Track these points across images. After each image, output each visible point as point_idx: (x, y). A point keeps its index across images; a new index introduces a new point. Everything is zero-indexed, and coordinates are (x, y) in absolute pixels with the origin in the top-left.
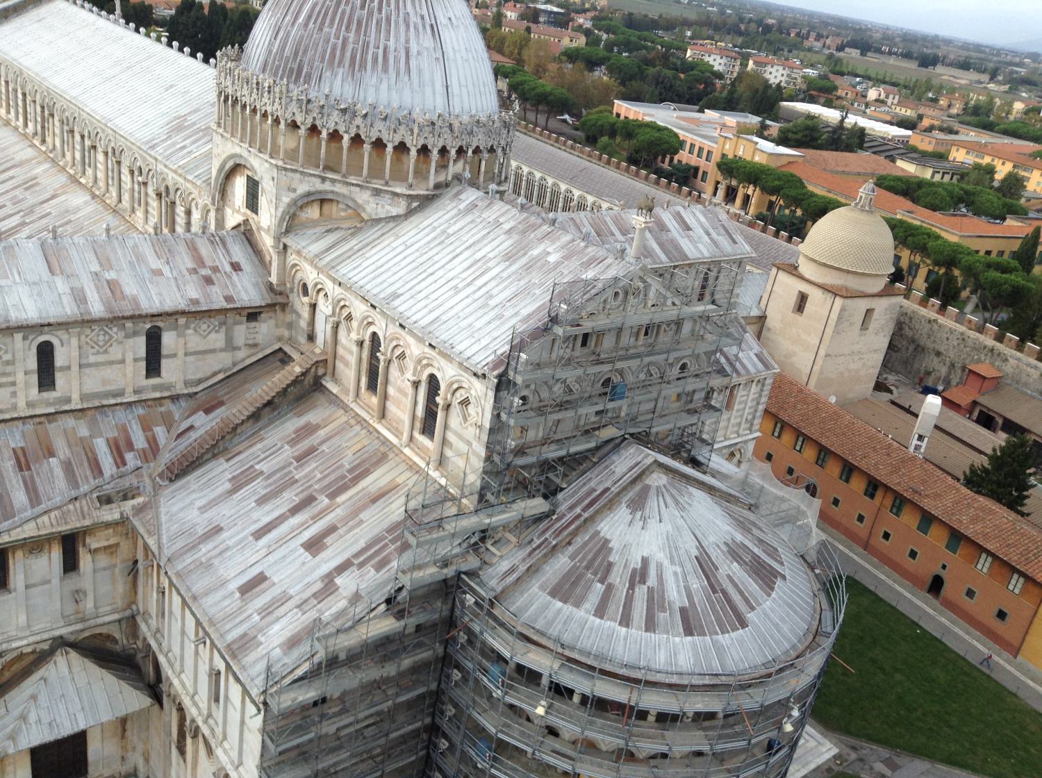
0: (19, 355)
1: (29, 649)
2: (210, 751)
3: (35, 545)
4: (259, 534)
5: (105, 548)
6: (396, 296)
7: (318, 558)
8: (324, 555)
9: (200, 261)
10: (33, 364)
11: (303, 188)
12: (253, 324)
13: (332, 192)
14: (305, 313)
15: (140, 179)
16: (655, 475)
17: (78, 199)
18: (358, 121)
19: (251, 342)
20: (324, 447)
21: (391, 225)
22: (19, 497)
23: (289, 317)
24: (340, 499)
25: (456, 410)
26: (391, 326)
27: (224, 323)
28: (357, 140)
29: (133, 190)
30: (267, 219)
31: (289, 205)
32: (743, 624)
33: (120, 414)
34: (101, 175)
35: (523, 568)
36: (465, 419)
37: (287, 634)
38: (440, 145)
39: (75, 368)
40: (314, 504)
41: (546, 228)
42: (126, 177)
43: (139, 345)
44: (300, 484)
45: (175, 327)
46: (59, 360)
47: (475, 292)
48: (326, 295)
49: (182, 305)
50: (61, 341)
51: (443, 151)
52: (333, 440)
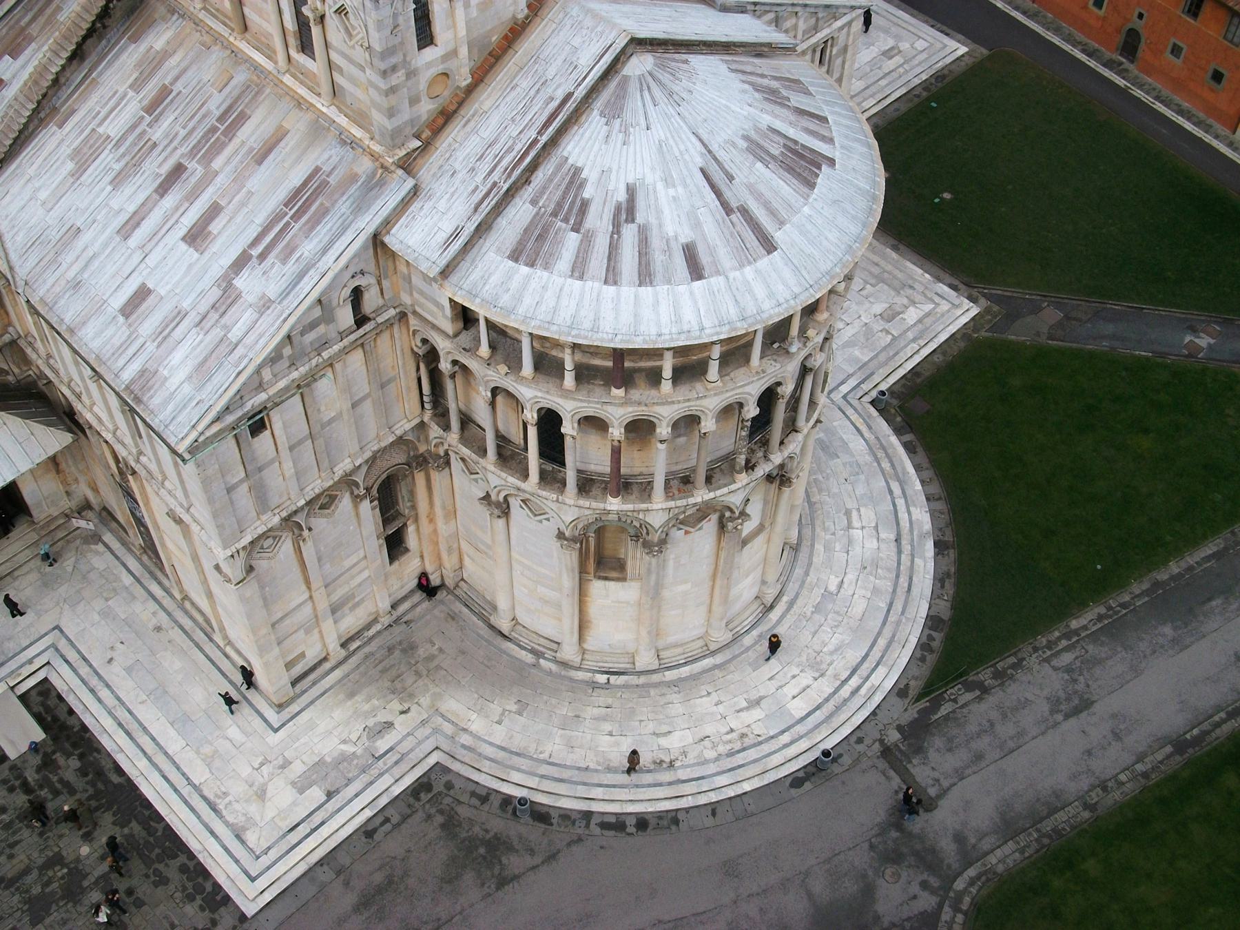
7: (207, 255)
8: (215, 247)
16: (634, 60)
20: (178, 87)
24: (217, 164)
25: (332, 21)
32: (769, 246)
35: (471, 227)
36: (350, 36)
40: (184, 176)
44: (160, 148)
52: (190, 73)
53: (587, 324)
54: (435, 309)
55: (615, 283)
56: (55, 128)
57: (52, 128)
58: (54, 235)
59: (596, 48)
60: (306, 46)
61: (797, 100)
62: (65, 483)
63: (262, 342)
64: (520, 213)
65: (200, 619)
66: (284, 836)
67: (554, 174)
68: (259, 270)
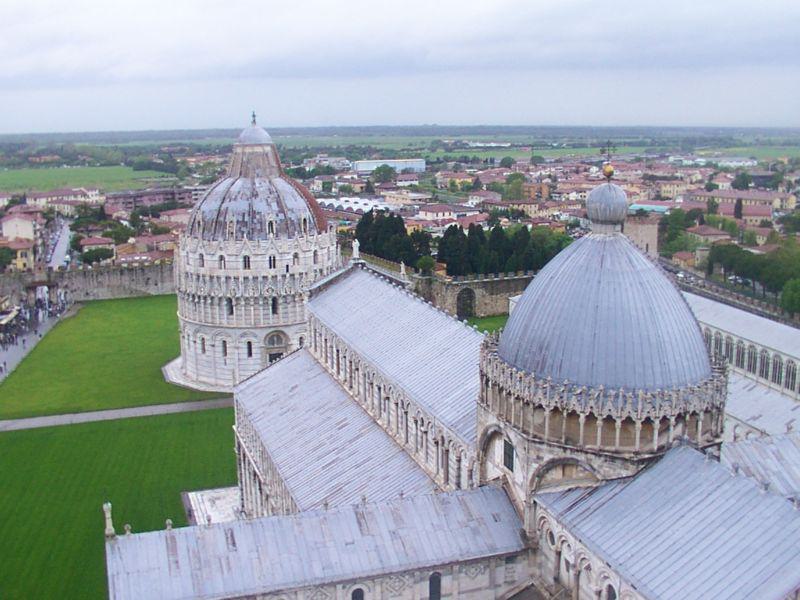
11: (547, 457)
12: (510, 566)
14: (553, 557)
15: (422, 429)
18: (592, 403)
19: (508, 579)
23: (540, 559)
26: (624, 584)
27: (488, 566)
28: (591, 418)
29: (417, 434)
30: (520, 476)
31: (538, 470)
38: (661, 416)
42: (412, 424)
48: (569, 545)
50: (369, 588)
51: (665, 420)
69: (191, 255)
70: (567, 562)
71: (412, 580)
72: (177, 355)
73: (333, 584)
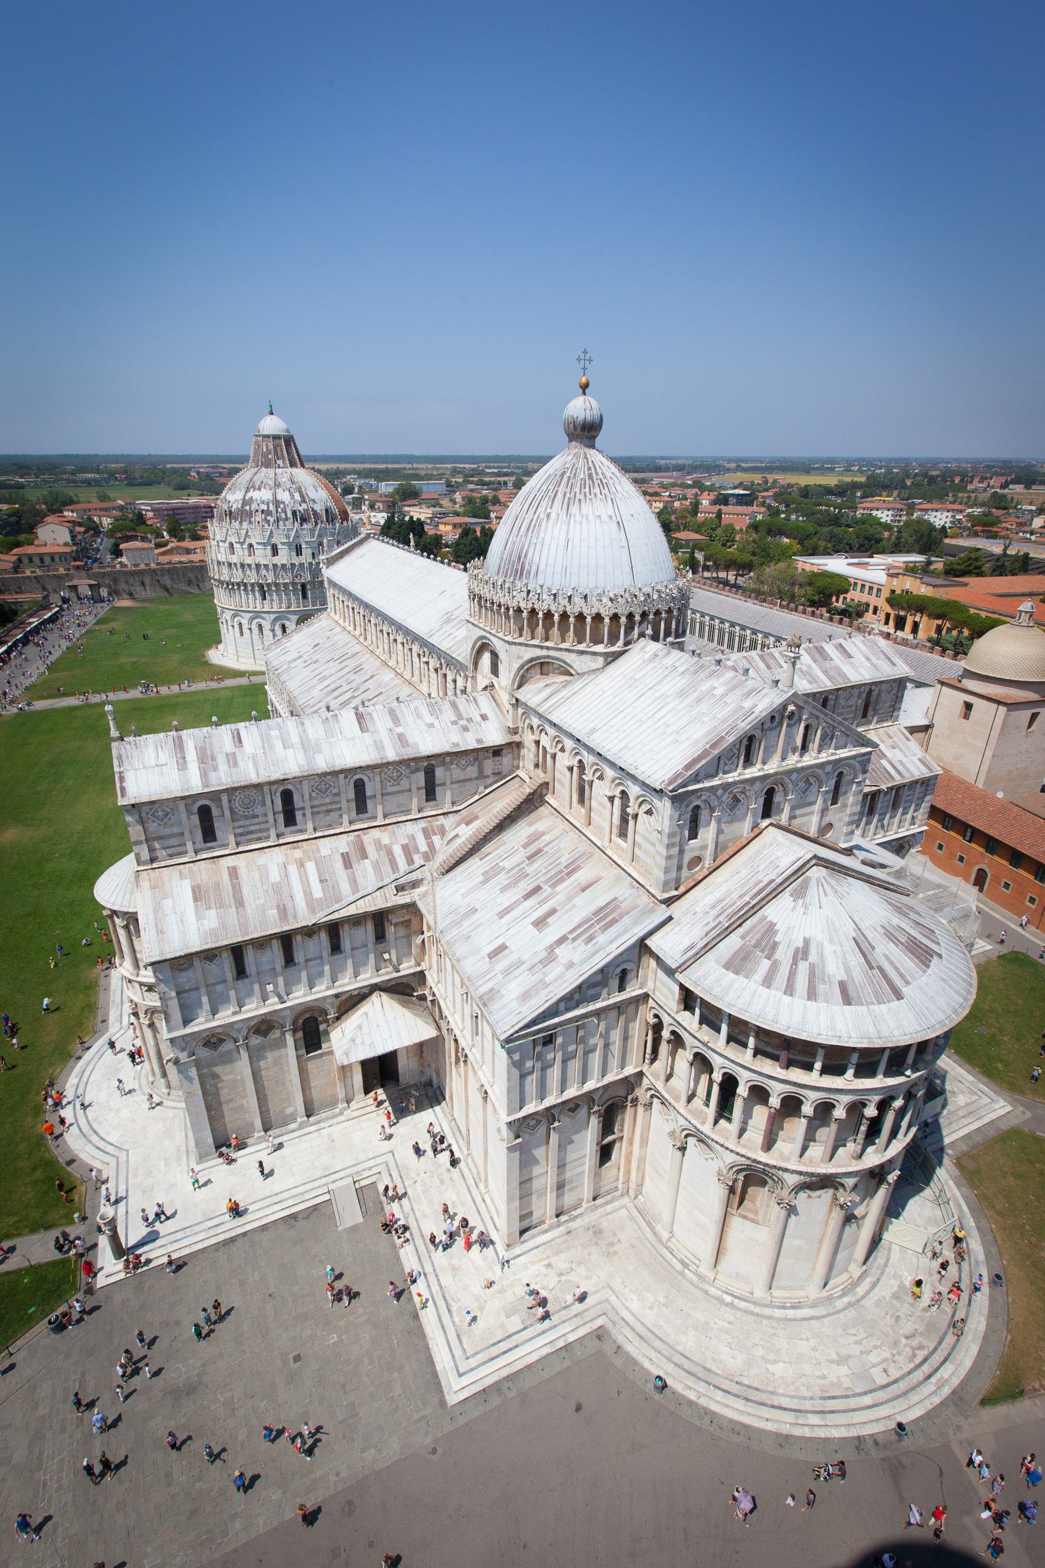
0: (343, 789)
1: (356, 993)
2: (475, 1073)
3: (357, 921)
4: (502, 914)
5: (402, 922)
6: (594, 730)
8: (547, 931)
9: (460, 717)
10: (352, 795)
12: (497, 758)
13: (548, 657)
17: (388, 676)
20: (546, 849)
21: (592, 677)
22: (345, 887)
24: (559, 888)
25: (642, 817)
28: (564, 616)
31: (519, 670)
33: (410, 828)
34: (400, 659)
35: (701, 944)
37: (521, 990)
39: (379, 797)
41: (714, 668)
42: (416, 659)
43: (420, 778)
45: (444, 764)
46: (369, 792)
47: (655, 724)
49: (447, 748)
51: (630, 616)
53: (770, 1017)
54: (668, 994)
55: (791, 995)
56: (477, 859)
57: (477, 859)
58: (463, 911)
59: (793, 858)
60: (623, 834)
61: (913, 916)
62: (422, 1065)
63: (564, 985)
64: (733, 942)
65: (475, 1171)
66: (488, 1348)
67: (758, 923)
68: (571, 946)
69: (221, 544)
70: (544, 748)
71: (408, 771)
72: (220, 642)
73: (335, 774)
